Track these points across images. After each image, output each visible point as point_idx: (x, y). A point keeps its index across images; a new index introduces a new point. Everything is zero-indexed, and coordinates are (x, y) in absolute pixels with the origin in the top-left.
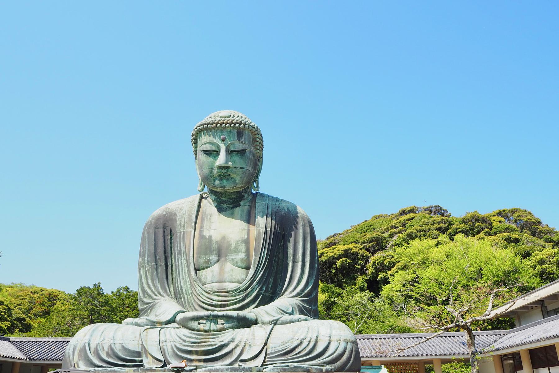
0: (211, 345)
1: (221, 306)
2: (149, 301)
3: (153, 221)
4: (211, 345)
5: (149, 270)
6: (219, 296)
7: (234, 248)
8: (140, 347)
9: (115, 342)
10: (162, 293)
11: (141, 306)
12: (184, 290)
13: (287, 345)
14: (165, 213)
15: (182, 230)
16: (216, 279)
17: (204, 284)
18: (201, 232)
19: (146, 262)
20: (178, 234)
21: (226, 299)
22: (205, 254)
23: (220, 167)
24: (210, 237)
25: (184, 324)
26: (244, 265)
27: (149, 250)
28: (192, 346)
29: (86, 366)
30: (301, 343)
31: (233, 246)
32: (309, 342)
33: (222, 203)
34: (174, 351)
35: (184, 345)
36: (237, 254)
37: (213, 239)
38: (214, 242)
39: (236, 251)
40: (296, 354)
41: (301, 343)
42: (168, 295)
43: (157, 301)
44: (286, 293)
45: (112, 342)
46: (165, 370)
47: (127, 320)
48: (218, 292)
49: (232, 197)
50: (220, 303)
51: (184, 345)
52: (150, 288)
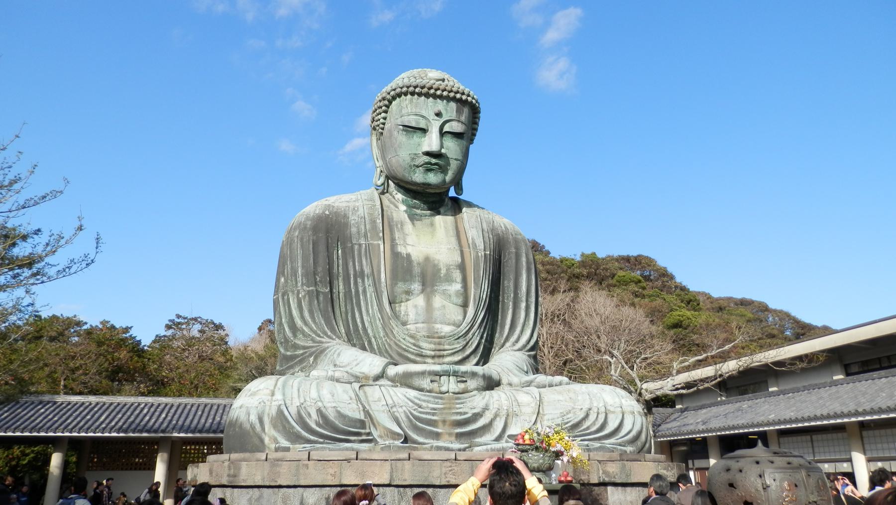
0: (461, 414)
1: (433, 357)
2: (306, 345)
3: (309, 223)
4: (461, 414)
5: (304, 297)
6: (430, 343)
7: (445, 275)
8: (362, 413)
9: (325, 404)
10: (329, 333)
11: (286, 350)
12: (370, 331)
13: (569, 416)
14: (327, 213)
15: (362, 242)
16: (421, 319)
17: (404, 324)
18: (393, 245)
19: (299, 284)
20: (356, 247)
21: (442, 347)
22: (405, 280)
23: (427, 154)
24: (409, 255)
25: (405, 380)
26: (460, 301)
27: (303, 267)
28: (433, 414)
29: (288, 440)
30: (587, 416)
31: (443, 271)
32: (598, 414)
33: (414, 207)
34: (410, 421)
35: (420, 412)
36: (450, 285)
37: (413, 258)
38: (415, 264)
39: (449, 279)
40: (584, 430)
41: (587, 416)
42: (339, 338)
43: (326, 345)
44: (508, 344)
45: (320, 404)
46: (432, 447)
47: (314, 373)
48: (428, 337)
49: (431, 200)
50: (433, 353)
51: (420, 412)
52: (306, 323)
